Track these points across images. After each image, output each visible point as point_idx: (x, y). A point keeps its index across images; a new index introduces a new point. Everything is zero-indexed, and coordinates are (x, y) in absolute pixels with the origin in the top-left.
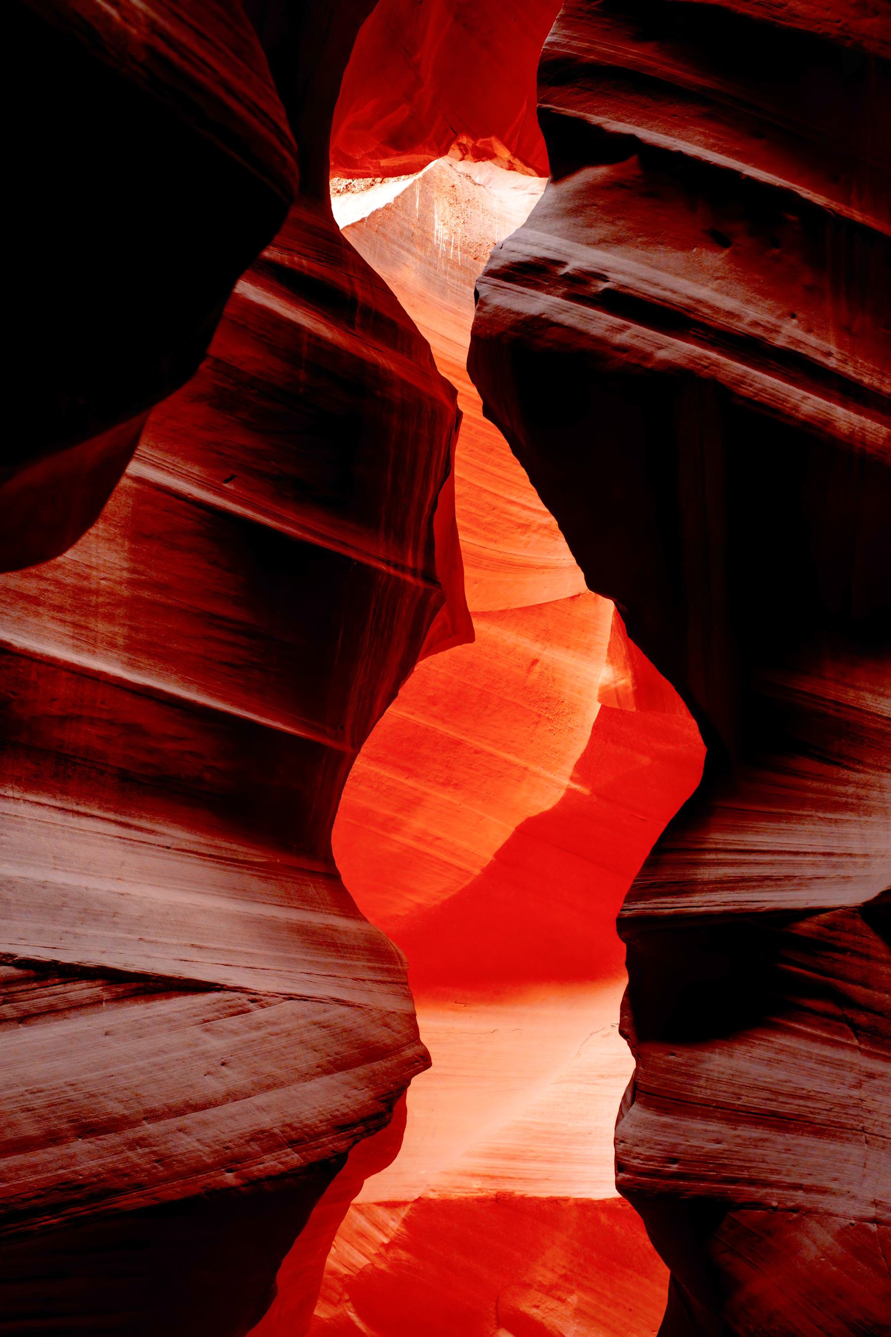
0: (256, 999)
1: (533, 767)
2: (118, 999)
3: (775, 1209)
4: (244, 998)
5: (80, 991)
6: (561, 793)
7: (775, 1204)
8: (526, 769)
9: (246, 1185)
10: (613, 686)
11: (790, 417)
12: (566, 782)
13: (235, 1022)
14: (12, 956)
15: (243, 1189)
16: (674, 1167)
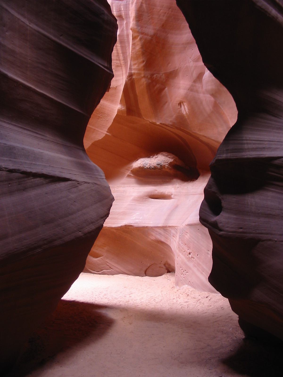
0: (79, 183)
1: (96, 129)
2: (47, 183)
3: (276, 241)
4: (76, 183)
5: (38, 180)
6: (104, 135)
7: (276, 240)
8: (95, 129)
9: (84, 235)
10: (121, 110)
11: (269, 14)
12: (106, 133)
13: (75, 190)
14: (19, 170)
15: (83, 236)
16: (241, 230)
